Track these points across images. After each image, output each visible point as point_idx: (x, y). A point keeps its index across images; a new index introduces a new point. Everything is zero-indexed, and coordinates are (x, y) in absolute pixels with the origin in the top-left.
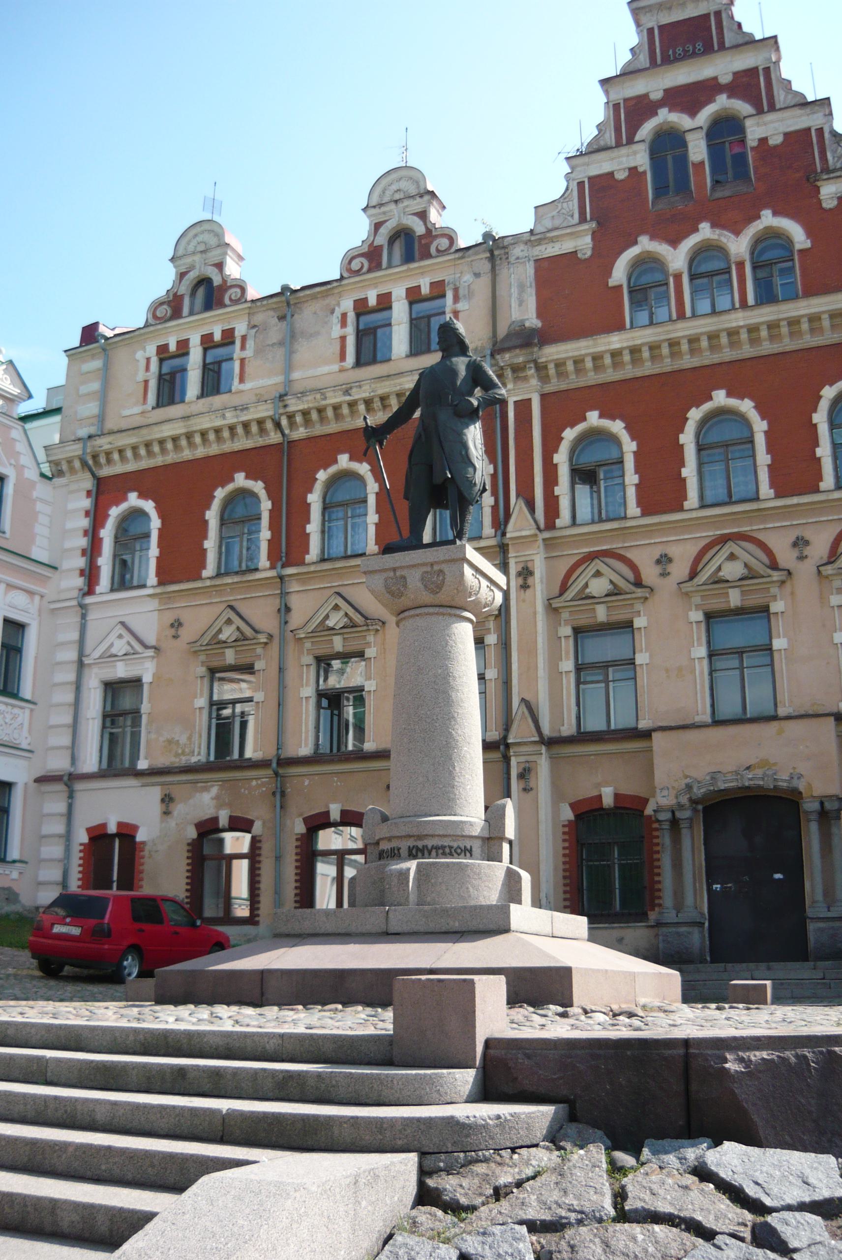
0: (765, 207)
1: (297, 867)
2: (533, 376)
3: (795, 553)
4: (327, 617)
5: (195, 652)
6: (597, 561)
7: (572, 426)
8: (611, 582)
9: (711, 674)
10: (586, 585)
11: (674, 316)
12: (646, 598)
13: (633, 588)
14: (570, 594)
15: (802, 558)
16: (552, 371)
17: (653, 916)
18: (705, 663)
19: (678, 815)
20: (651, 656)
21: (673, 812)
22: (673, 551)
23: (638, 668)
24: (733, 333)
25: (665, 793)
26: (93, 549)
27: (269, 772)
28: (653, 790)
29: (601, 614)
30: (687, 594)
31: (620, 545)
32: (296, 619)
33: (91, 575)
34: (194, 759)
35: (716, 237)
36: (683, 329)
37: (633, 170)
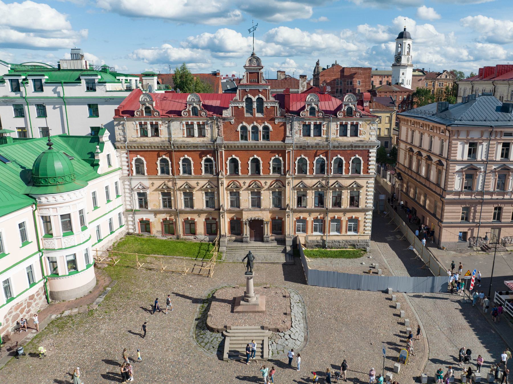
26: (129, 166)
32: (178, 186)
33: (130, 170)
37: (242, 107)
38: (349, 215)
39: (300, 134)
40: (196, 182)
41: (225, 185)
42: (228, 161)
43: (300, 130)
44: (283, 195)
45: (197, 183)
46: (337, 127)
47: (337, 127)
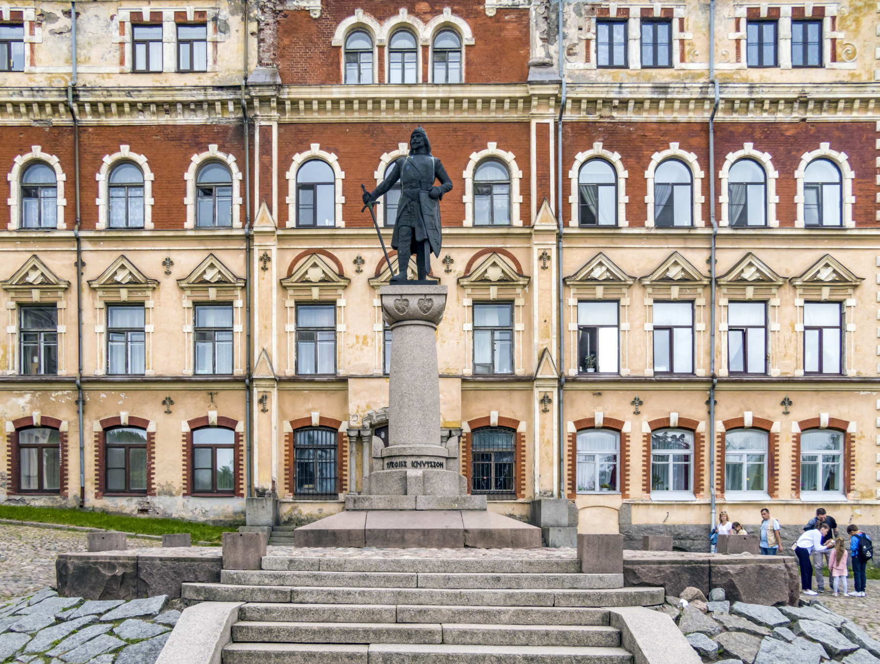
0: (449, 5)
1: (96, 456)
2: (273, 108)
3: (444, 268)
4: (115, 273)
5: (6, 290)
6: (315, 256)
7: (300, 152)
8: (323, 272)
9: (384, 343)
10: (306, 272)
11: (376, 81)
12: (346, 287)
13: (339, 279)
14: (295, 278)
15: (448, 271)
16: (288, 107)
17: (342, 496)
18: (381, 334)
19: (362, 433)
20: (348, 327)
21: (359, 431)
22: (365, 255)
23: (338, 335)
24: (417, 101)
25: (355, 418)
27: (74, 386)
28: (347, 417)
29: (315, 294)
30: (373, 287)
31: (330, 246)
32: (90, 273)
34: (10, 372)
35: (410, 22)
36: (384, 92)
38: (808, 407)
39: (588, 60)
40: (161, 257)
41: (277, 270)
42: (294, 167)
43: (588, 41)
44: (519, 314)
45: (168, 263)
46: (738, 29)
47: (738, 29)
